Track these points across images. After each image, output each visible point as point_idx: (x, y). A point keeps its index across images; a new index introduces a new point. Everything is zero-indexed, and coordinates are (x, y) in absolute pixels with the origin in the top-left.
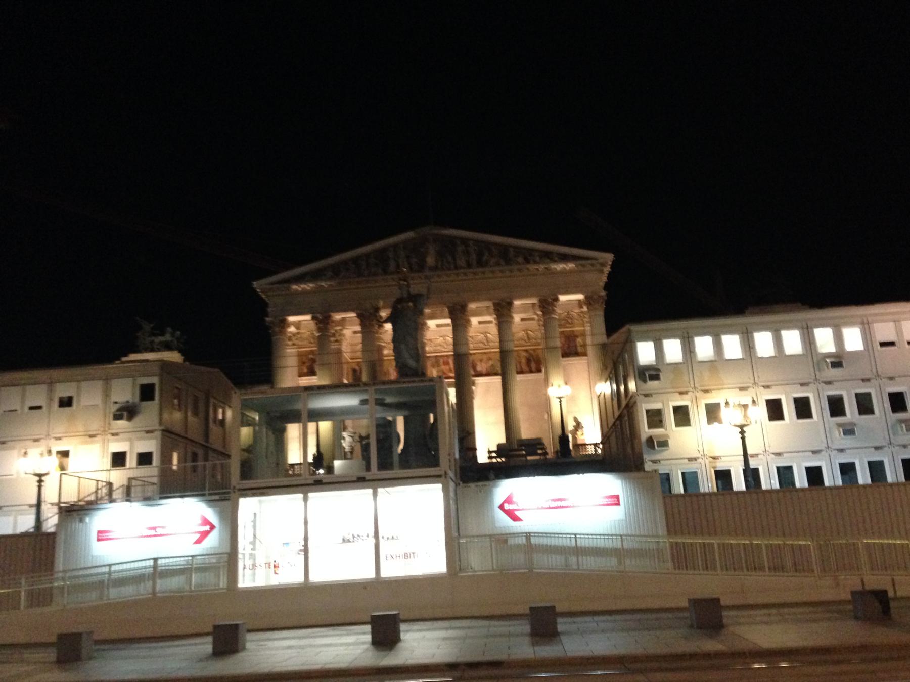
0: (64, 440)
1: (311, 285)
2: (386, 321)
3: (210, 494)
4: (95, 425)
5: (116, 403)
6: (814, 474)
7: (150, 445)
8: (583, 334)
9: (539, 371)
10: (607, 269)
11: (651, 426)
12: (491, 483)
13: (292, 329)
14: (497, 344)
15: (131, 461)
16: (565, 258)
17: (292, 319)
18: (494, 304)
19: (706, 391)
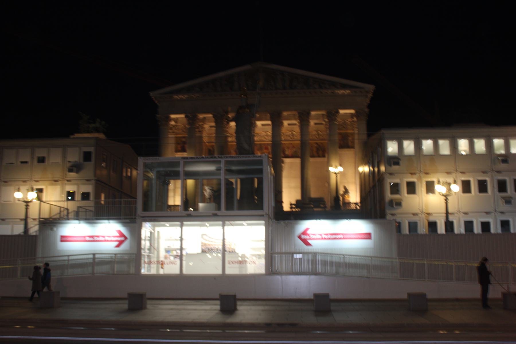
0: (41, 183)
1: (186, 96)
2: (232, 121)
3: (125, 219)
4: (58, 175)
5: (70, 162)
6: (485, 226)
7: (88, 188)
8: (353, 134)
9: (324, 156)
10: (370, 95)
11: (392, 193)
12: (293, 222)
13: (173, 123)
14: (299, 137)
15: (78, 197)
16: (344, 87)
17: (173, 116)
18: (299, 113)
19: (427, 173)
